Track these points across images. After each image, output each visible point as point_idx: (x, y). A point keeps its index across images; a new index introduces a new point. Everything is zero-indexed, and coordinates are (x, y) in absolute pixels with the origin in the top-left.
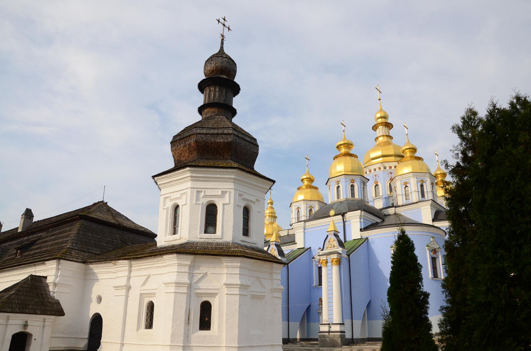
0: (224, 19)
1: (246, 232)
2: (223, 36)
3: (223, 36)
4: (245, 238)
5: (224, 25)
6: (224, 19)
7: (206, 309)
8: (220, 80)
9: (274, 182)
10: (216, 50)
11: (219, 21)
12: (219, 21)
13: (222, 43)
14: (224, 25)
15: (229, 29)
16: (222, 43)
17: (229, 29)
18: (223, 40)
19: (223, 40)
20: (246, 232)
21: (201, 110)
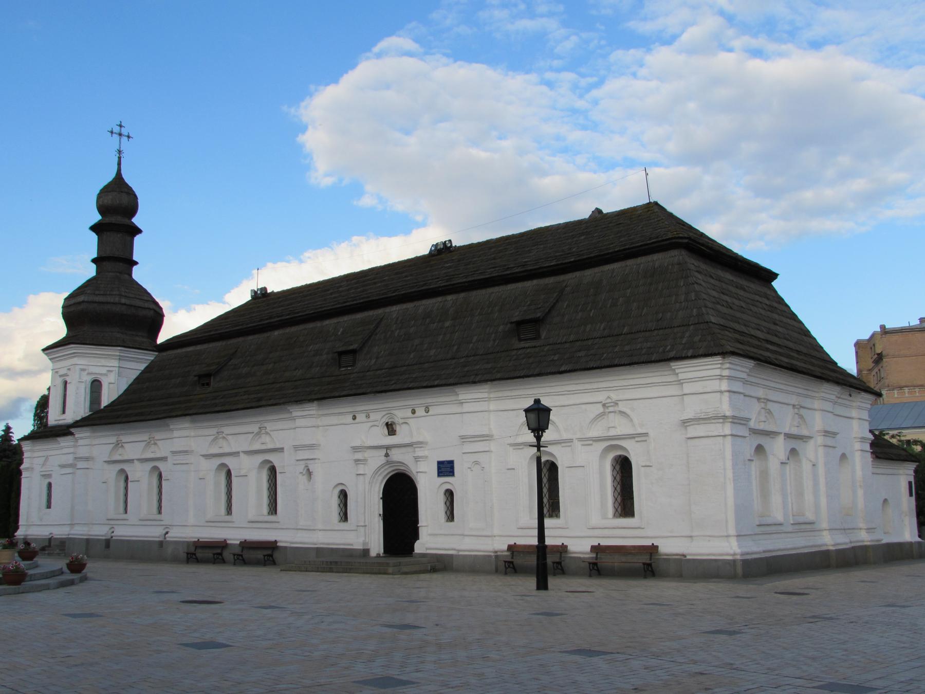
0: (121, 126)
2: (120, 152)
3: (120, 152)
5: (120, 135)
6: (121, 126)
8: (117, 217)
10: (110, 176)
11: (112, 132)
12: (112, 132)
13: (119, 164)
14: (120, 135)
15: (129, 137)
16: (119, 164)
17: (129, 137)
18: (120, 158)
19: (120, 158)
21: (94, 261)
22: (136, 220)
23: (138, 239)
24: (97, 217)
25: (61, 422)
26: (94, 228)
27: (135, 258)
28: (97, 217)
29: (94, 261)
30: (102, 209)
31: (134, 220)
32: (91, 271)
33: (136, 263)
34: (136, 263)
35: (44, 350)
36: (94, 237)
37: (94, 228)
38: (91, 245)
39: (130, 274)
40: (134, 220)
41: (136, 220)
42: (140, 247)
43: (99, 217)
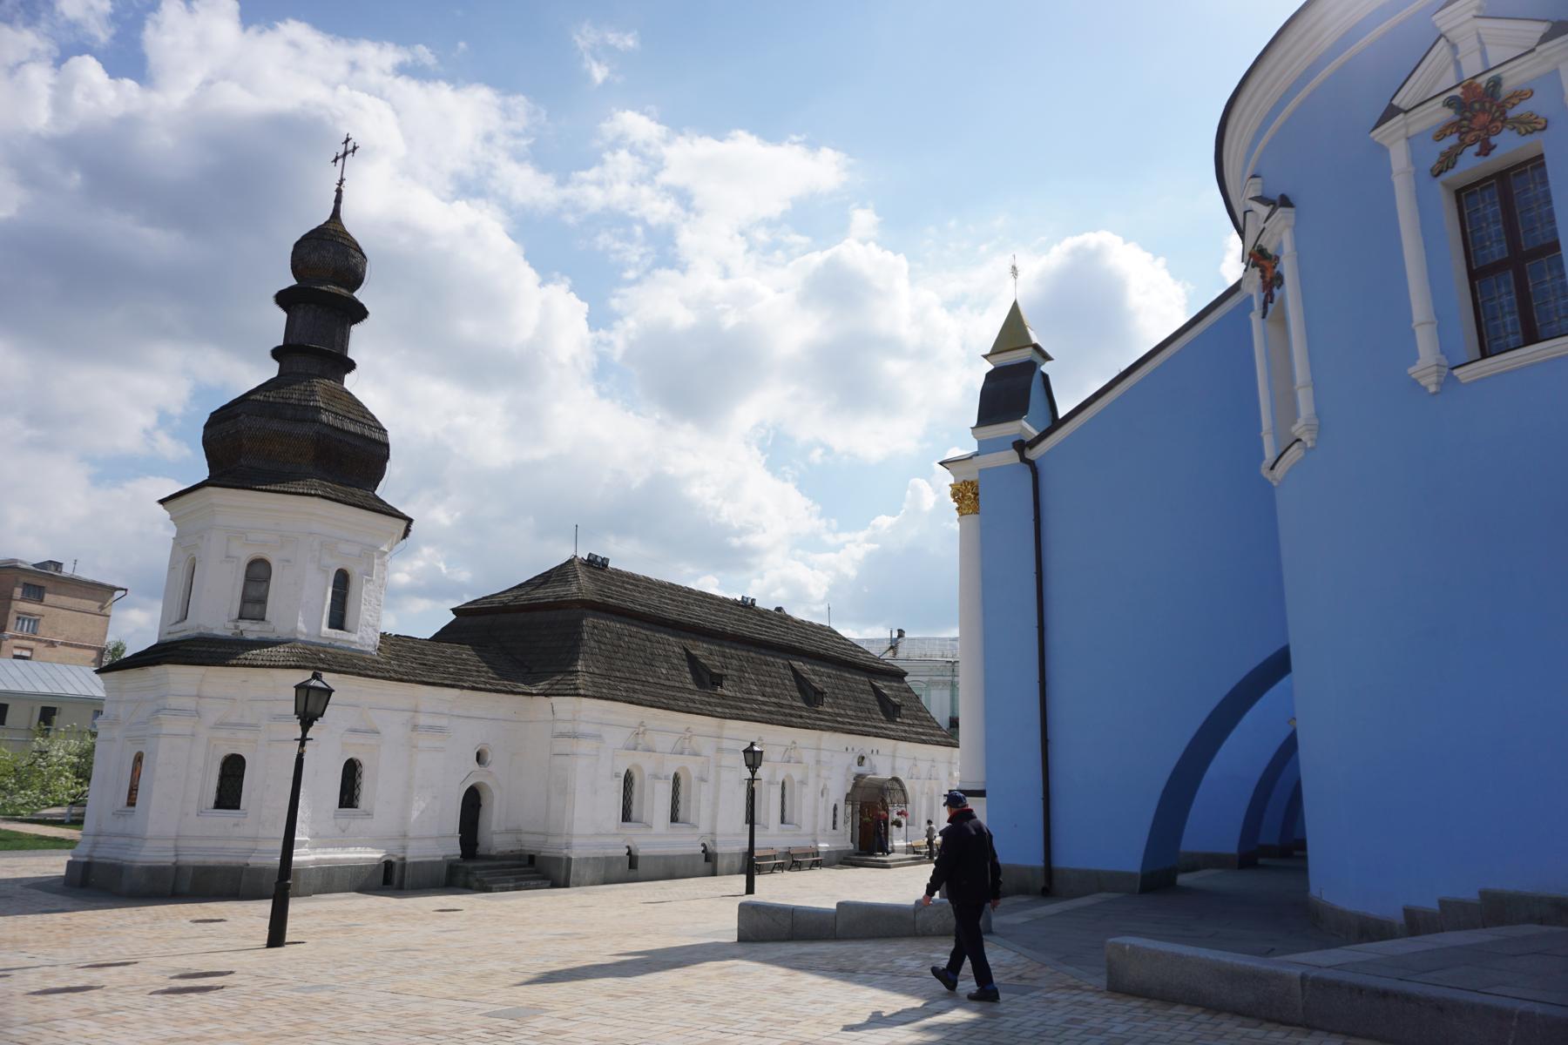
1: (338, 620)
4: (335, 633)
7: (233, 769)
9: (410, 521)
10: (323, 217)
13: (338, 201)
16: (338, 201)
18: (339, 192)
19: (339, 192)
20: (338, 620)
21: (277, 353)
22: (360, 295)
25: (175, 637)
26: (283, 299)
27: (350, 356)
29: (277, 353)
31: (356, 294)
32: (271, 370)
33: (351, 366)
35: (162, 502)
37: (283, 299)
38: (275, 324)
40: (356, 294)
41: (360, 295)
42: (360, 342)
43: (295, 282)
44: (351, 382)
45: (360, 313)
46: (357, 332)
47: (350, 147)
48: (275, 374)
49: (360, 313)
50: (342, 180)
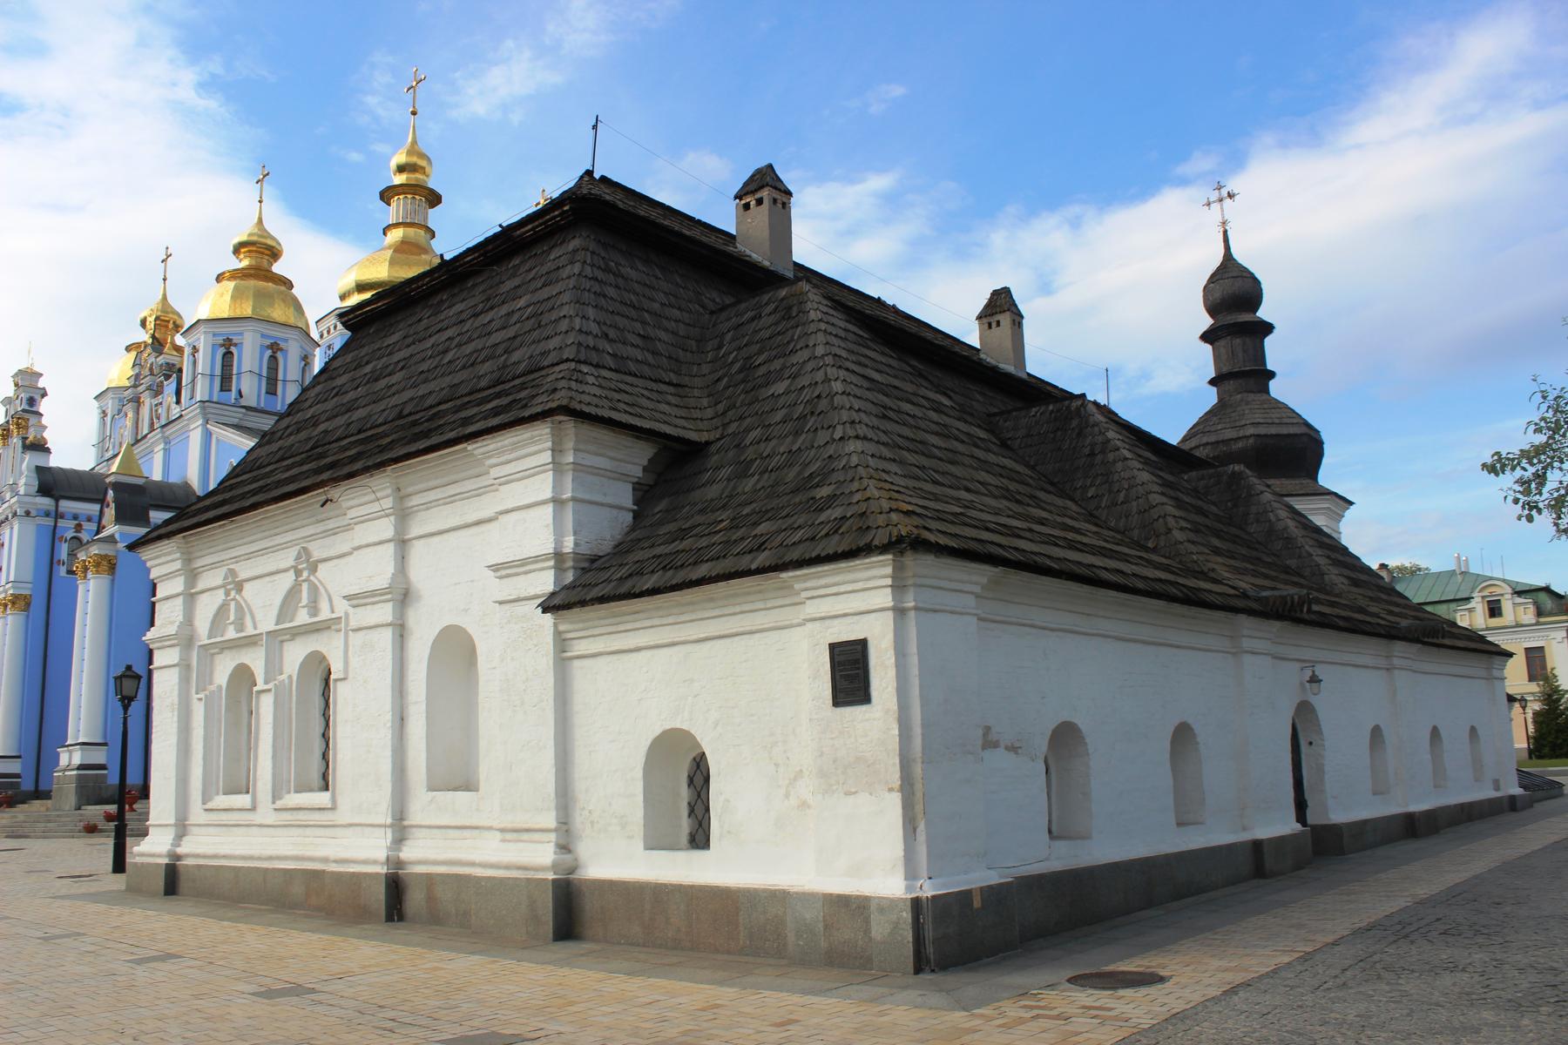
10: (1216, 259)
18: (1225, 232)
19: (1225, 232)
21: (1212, 382)
22: (1263, 313)
23: (1269, 342)
24: (1206, 322)
26: (1206, 337)
27: (1270, 367)
28: (1206, 322)
29: (1212, 382)
30: (1212, 310)
33: (1272, 375)
34: (1272, 375)
36: (1208, 349)
37: (1206, 337)
39: (1267, 391)
42: (1275, 351)
44: (1276, 389)
45: (1267, 328)
46: (1268, 341)
47: (1224, 192)
48: (1214, 400)
49: (1267, 328)
50: (1224, 223)
